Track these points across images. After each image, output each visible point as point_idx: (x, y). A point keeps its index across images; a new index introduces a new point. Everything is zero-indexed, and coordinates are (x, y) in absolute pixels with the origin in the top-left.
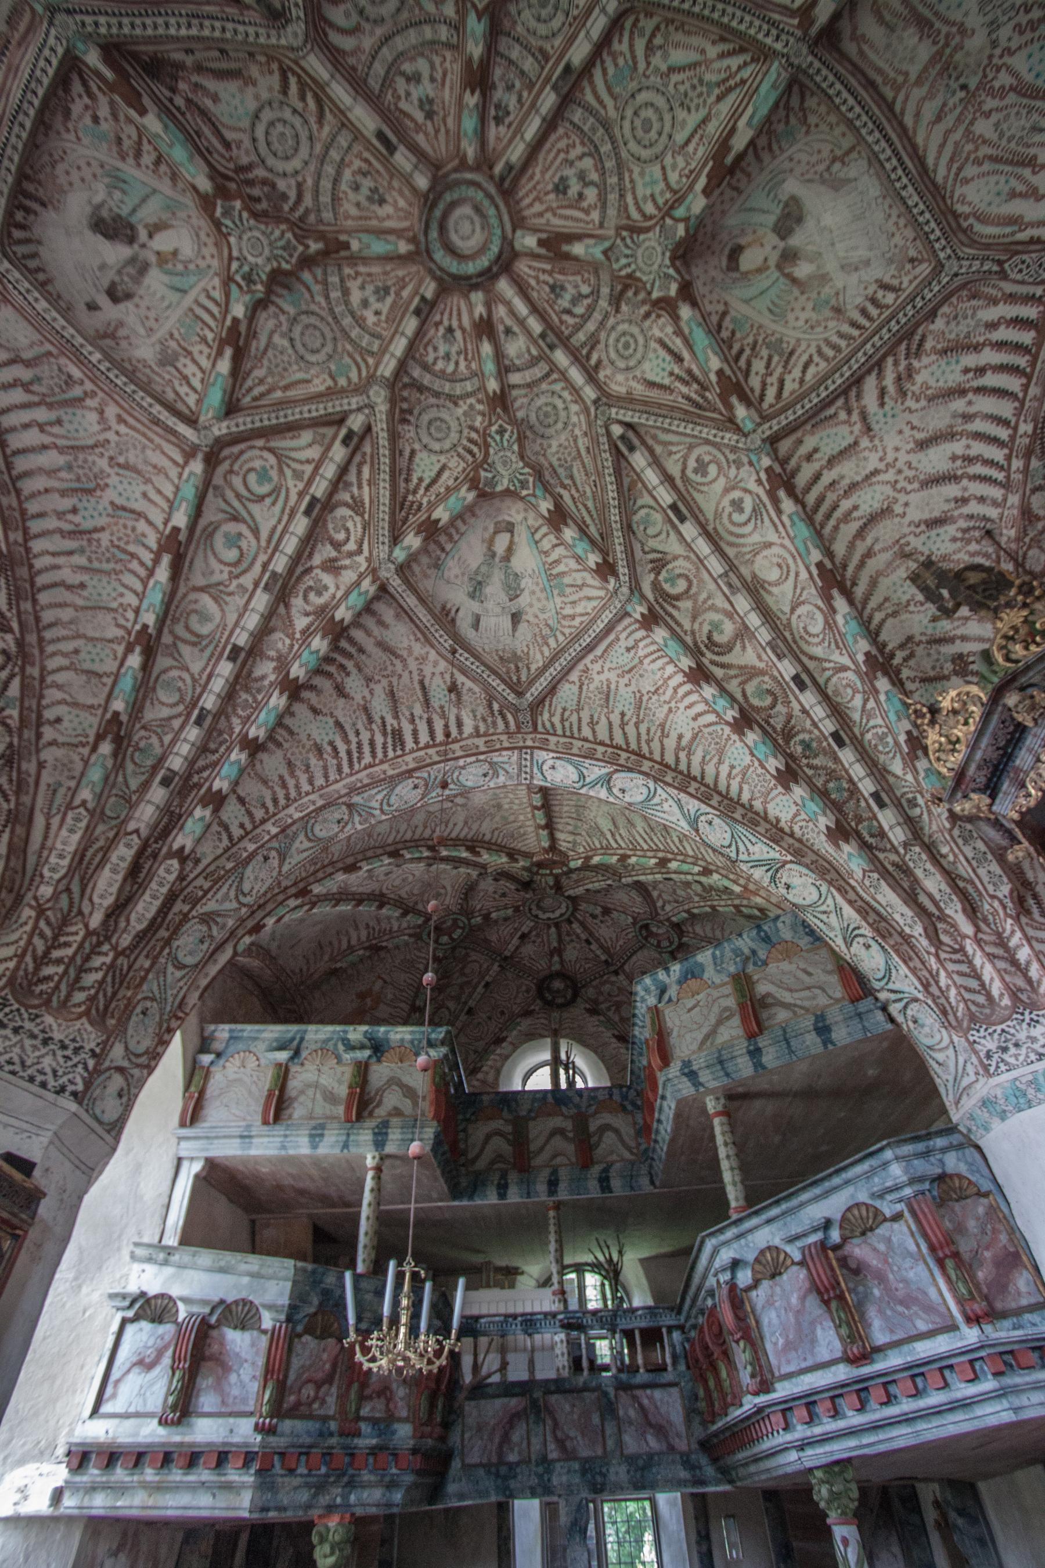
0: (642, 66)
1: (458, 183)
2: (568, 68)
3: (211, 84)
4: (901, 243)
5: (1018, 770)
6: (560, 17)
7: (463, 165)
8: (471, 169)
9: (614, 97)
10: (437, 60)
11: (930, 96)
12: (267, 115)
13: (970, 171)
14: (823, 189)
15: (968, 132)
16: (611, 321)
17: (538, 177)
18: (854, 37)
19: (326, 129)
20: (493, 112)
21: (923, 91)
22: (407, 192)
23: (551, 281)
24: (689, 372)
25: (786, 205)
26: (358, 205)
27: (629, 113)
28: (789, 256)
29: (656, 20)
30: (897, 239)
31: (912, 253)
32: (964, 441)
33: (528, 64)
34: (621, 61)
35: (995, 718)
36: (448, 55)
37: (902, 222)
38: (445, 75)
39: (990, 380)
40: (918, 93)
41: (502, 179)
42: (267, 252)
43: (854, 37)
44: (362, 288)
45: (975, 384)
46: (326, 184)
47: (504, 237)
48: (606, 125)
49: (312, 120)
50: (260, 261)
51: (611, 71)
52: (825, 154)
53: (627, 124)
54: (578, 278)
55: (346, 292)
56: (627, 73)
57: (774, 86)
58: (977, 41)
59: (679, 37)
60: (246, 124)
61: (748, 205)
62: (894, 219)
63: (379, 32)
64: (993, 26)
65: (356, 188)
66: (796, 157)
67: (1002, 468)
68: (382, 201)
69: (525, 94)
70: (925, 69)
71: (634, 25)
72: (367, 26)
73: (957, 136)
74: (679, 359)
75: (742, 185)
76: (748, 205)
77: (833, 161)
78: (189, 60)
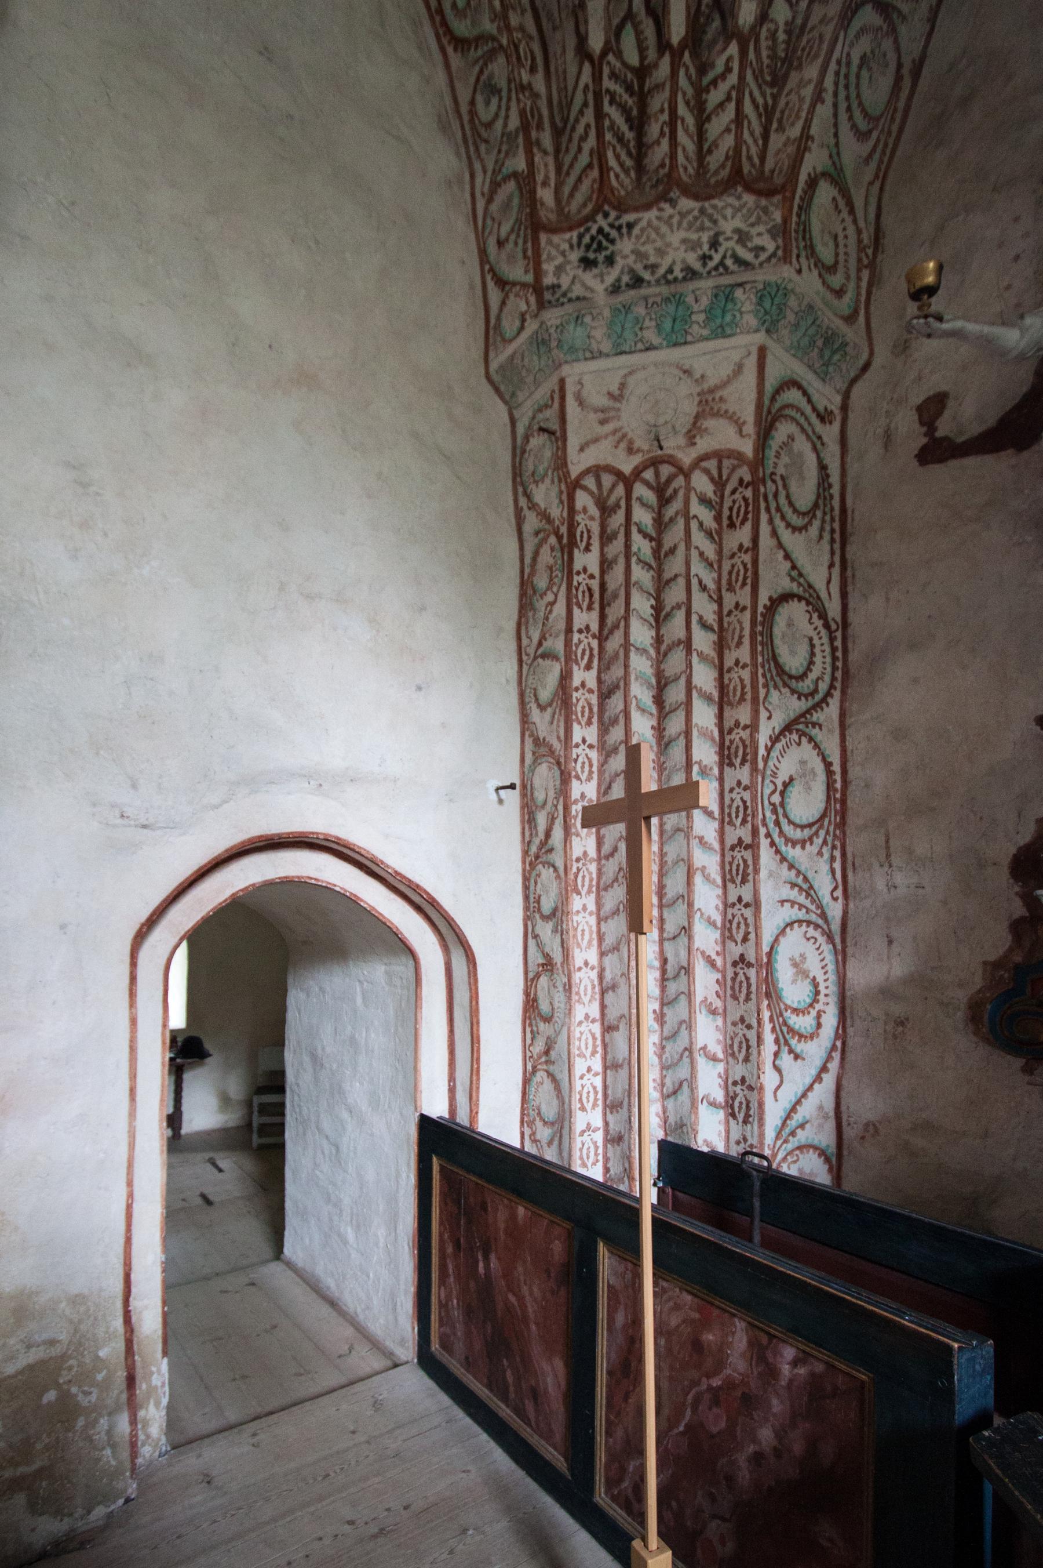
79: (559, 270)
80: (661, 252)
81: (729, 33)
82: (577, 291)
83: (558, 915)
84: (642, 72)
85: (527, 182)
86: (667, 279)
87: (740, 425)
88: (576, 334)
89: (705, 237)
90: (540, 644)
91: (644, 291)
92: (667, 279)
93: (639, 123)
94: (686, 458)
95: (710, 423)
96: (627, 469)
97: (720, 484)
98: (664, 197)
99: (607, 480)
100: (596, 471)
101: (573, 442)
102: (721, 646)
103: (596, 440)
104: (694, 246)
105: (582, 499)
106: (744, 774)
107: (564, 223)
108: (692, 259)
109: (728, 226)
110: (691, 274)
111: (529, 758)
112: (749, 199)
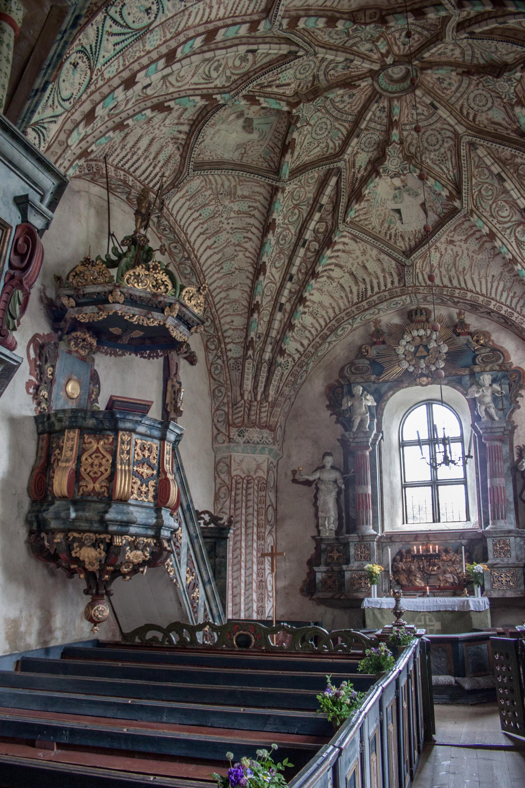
0: (329, 141)
1: (402, 91)
2: (358, 136)
3: (504, 123)
4: (206, 154)
5: (179, 326)
6: (363, 142)
7: (398, 98)
8: (395, 97)
9: (338, 128)
10: (410, 119)
11: (229, 187)
12: (485, 109)
13: (203, 183)
14: (243, 142)
15: (211, 188)
16: (315, 70)
17: (363, 96)
18: (263, 186)
19: (460, 103)
20: (386, 110)
21: (232, 186)
22: (426, 83)
23: (350, 69)
24: (271, 86)
25: (252, 129)
26: (450, 78)
27: (329, 127)
28: (241, 114)
29: (328, 153)
30: (208, 153)
31: (201, 156)
32: (141, 154)
33: (373, 125)
34: (337, 138)
35: (195, 319)
36: (406, 122)
37: (211, 158)
38: (407, 116)
39: (151, 168)
40: (233, 184)
41: (380, 97)
42: (497, 84)
43: (263, 186)
44: (452, 55)
45: (153, 164)
46: (464, 85)
47: (377, 81)
48: (337, 119)
49: (466, 105)
50: (502, 83)
51: (340, 135)
52: (250, 152)
53: (328, 123)
54: (336, 75)
55: (463, 53)
56: (334, 137)
57: (285, 174)
58: (227, 203)
59: (318, 154)
60: (494, 108)
61: (270, 126)
62: (214, 156)
63: (434, 127)
64: (225, 207)
65: (450, 84)
66: (260, 147)
67: (122, 166)
68: (439, 79)
69: (373, 117)
70: (236, 190)
71: (335, 149)
72: (438, 129)
73: (214, 186)
74: (278, 86)
75: (277, 134)
76: (270, 126)
77: (245, 152)
78: (509, 132)
79: (234, 435)
81: (267, 401)
82: (237, 441)
84: (251, 401)
85: (227, 414)
86: (254, 443)
87: (264, 472)
88: (236, 448)
92: (254, 443)
93: (249, 410)
94: (254, 477)
95: (258, 470)
96: (243, 477)
97: (259, 481)
98: (253, 427)
99: (238, 478)
100: (237, 476)
101: (233, 469)
102: (258, 515)
104: (259, 438)
105: (234, 481)
106: (263, 542)
107: (234, 425)
109: (265, 435)
110: (258, 443)
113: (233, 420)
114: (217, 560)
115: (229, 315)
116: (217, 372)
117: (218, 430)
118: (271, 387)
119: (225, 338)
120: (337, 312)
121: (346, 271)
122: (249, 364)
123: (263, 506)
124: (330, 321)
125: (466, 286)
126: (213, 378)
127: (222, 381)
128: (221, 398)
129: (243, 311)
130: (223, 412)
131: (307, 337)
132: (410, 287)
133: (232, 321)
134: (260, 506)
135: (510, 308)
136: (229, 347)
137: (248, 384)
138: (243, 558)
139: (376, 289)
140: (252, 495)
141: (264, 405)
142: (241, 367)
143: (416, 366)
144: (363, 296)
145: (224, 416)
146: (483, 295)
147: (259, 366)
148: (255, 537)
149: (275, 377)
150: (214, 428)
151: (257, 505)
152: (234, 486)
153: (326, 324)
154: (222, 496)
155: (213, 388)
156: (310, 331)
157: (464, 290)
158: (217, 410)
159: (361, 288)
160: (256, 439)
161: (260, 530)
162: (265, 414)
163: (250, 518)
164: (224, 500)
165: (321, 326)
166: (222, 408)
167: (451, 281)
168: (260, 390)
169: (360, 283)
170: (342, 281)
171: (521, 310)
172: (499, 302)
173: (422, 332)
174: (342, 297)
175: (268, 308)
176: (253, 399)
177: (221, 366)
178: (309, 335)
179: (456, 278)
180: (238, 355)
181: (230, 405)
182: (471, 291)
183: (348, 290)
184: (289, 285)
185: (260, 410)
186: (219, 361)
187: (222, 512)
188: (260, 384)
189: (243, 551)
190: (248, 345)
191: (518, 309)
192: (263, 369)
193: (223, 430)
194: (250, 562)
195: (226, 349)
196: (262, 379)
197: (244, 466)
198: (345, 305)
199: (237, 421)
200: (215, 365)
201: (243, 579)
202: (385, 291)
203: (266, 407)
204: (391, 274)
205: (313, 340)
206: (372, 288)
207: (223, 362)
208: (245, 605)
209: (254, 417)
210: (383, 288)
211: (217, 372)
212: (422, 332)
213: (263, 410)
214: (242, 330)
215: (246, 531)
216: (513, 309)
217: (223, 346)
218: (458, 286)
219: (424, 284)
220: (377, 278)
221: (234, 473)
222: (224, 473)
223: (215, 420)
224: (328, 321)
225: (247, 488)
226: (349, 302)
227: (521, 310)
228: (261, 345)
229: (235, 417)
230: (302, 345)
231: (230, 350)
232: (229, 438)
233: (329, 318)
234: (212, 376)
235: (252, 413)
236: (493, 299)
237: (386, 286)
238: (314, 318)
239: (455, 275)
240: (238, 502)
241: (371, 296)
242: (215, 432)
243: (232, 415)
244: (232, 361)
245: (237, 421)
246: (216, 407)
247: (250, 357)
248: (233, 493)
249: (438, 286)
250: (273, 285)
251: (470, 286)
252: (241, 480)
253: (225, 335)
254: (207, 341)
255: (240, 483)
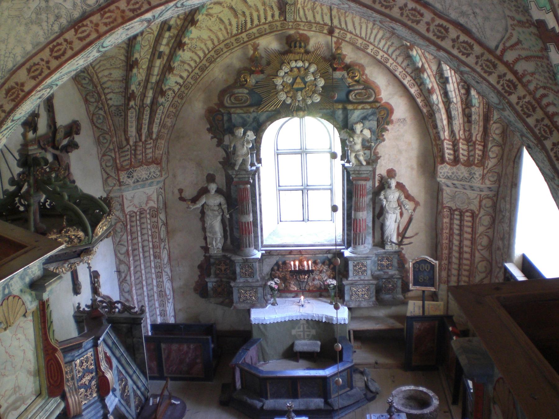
79: (123, 178)
80: (141, 175)
81: (151, 139)
82: (127, 183)
83: (130, 292)
85: (115, 160)
86: (142, 181)
87: (154, 202)
89: (148, 173)
90: (119, 242)
91: (140, 183)
92: (142, 181)
94: (146, 208)
95: (150, 202)
96: (136, 211)
97: (150, 210)
98: (141, 165)
101: (126, 206)
102: (152, 238)
103: (130, 206)
104: (147, 174)
105: (128, 216)
106: (159, 261)
107: (122, 169)
108: (147, 177)
109: (152, 170)
110: (147, 179)
111: (118, 263)
112: (155, 165)
113: (120, 163)
114: (135, 340)
115: (107, 69)
116: (100, 121)
117: (108, 174)
118: (154, 125)
119: (103, 89)
120: (216, 43)
121: (225, 6)
122: (132, 113)
123: (157, 230)
124: (209, 52)
125: (347, 27)
126: (96, 127)
127: (105, 129)
128: (107, 145)
129: (121, 65)
130: (110, 158)
131: (186, 70)
132: (291, 22)
133: (111, 74)
134: (153, 230)
135: (387, 54)
136: (109, 96)
137: (132, 131)
138: (144, 278)
139: (256, 22)
140: (146, 224)
141: (149, 142)
142: (123, 114)
143: (294, 98)
144: (243, 28)
145: (111, 161)
146: (362, 38)
147: (142, 110)
148: (152, 258)
149: (157, 116)
150: (103, 172)
151: (151, 230)
152: (128, 220)
153: (205, 55)
154: (119, 230)
155: (97, 135)
156: (189, 64)
157: (344, 30)
158: (104, 155)
159: (240, 20)
160: (144, 176)
161: (155, 250)
162: (151, 150)
163: (146, 243)
164: (121, 234)
165: (200, 58)
166: (109, 153)
167: (331, 20)
168: (144, 131)
169: (239, 16)
170: (220, 15)
171: (397, 58)
172: (377, 47)
173: (300, 64)
174: (221, 29)
175: (147, 56)
176: (138, 140)
177: (104, 116)
178: (186, 67)
179: (337, 17)
180: (119, 103)
181: (117, 150)
182: (351, 33)
183: (227, 22)
184: (167, 34)
185: (145, 147)
186: (101, 112)
187: (121, 245)
188: (143, 126)
189: (143, 272)
190: (129, 96)
191: (394, 56)
192: (145, 113)
193: (113, 175)
194: (150, 279)
195: (106, 98)
196: (146, 121)
197: (136, 202)
198: (224, 36)
199: (125, 164)
200: (97, 116)
201: (146, 294)
202: (265, 24)
203: (150, 144)
204: (272, 8)
205: (192, 71)
206: (252, 21)
207: (105, 112)
208: (150, 312)
209: (140, 157)
210: (263, 21)
211: (100, 121)
212: (300, 64)
213: (148, 146)
214: (121, 81)
215: (143, 255)
216: (388, 55)
217: (103, 97)
218: (339, 26)
219: (304, 20)
220: (258, 10)
221: (127, 210)
222: (118, 211)
223: (104, 164)
224: (207, 52)
225: (141, 224)
226: (228, 33)
227: (397, 58)
228: (141, 90)
229: (122, 159)
230: (181, 77)
231: (111, 99)
232: (120, 182)
233: (208, 49)
234: (95, 125)
235: (138, 152)
236: (371, 43)
237: (266, 19)
238: (193, 52)
239: (337, 15)
240: (134, 233)
241: (250, 29)
242: (105, 176)
243: (120, 158)
244: (113, 109)
245: (125, 164)
246: (102, 153)
247: (132, 107)
248: (129, 227)
249: (318, 23)
250: (152, 35)
251: (350, 28)
252: (134, 214)
253: (104, 86)
254: (87, 95)
255: (133, 217)
